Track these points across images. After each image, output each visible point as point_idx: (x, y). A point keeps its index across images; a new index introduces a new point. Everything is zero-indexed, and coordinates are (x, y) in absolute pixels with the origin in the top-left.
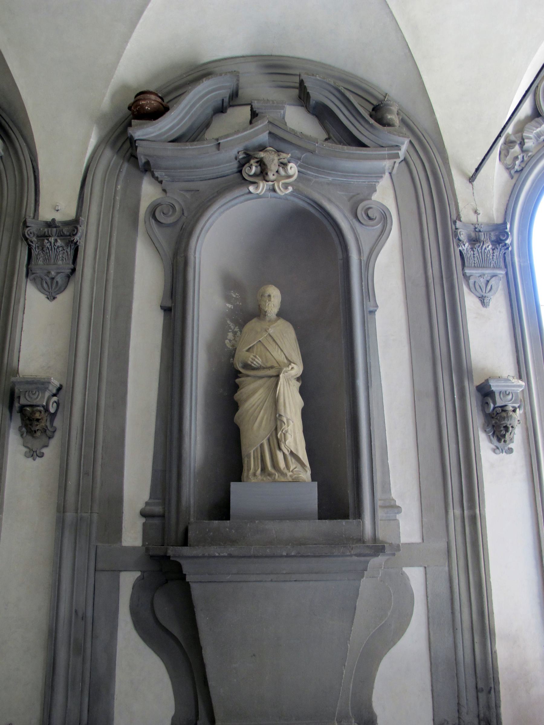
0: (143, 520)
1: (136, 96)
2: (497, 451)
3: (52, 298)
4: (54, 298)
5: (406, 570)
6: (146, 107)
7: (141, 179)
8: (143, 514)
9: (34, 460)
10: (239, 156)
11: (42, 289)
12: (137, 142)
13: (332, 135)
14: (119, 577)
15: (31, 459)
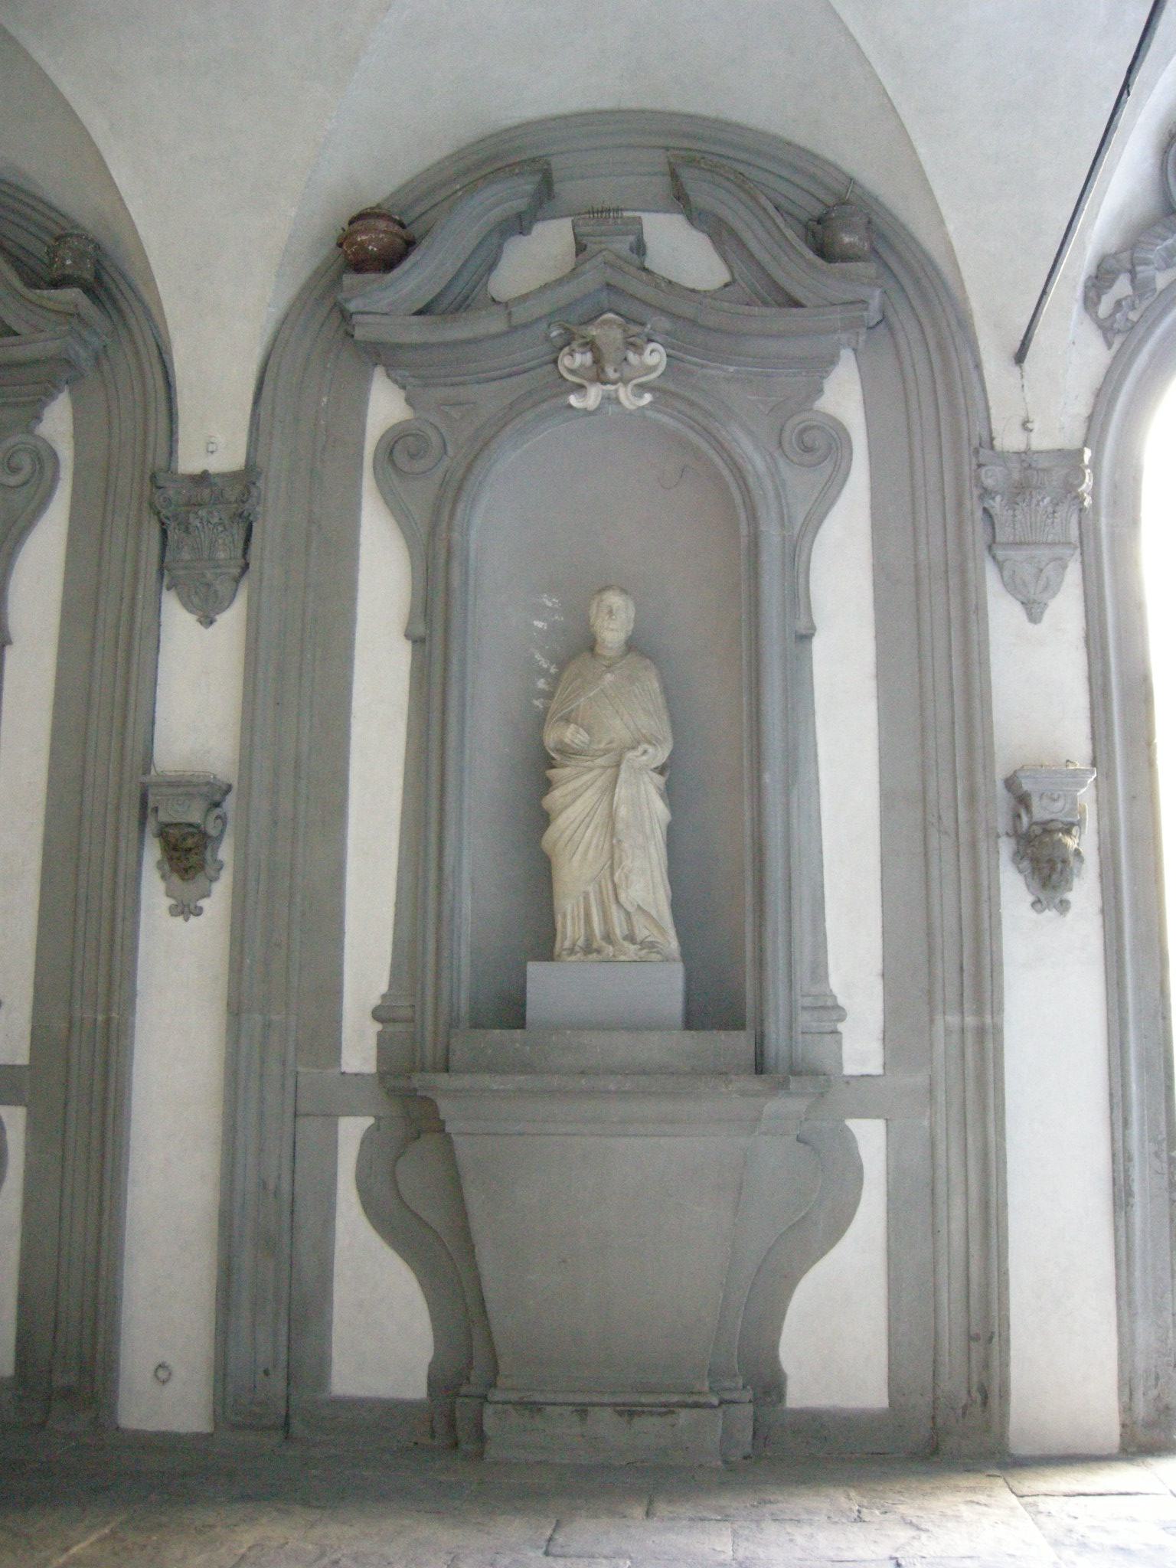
0: (378, 1027)
1: (351, 223)
2: (1039, 906)
3: (207, 621)
4: (211, 622)
5: (853, 1124)
6: (369, 245)
7: (367, 380)
8: (377, 1015)
9: (186, 920)
10: (551, 332)
11: (188, 605)
12: (354, 316)
13: (737, 276)
14: (336, 1125)
15: (180, 919)
